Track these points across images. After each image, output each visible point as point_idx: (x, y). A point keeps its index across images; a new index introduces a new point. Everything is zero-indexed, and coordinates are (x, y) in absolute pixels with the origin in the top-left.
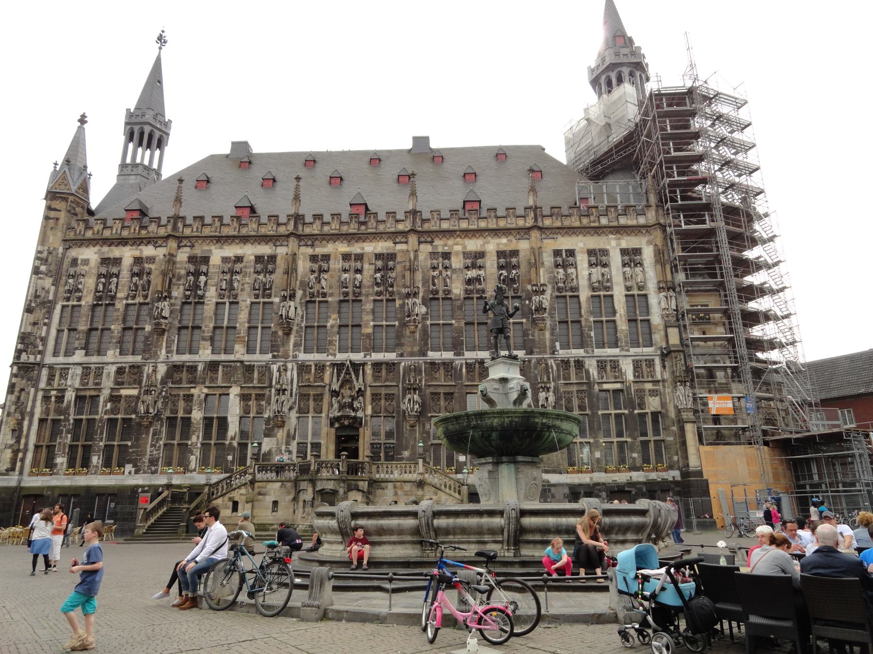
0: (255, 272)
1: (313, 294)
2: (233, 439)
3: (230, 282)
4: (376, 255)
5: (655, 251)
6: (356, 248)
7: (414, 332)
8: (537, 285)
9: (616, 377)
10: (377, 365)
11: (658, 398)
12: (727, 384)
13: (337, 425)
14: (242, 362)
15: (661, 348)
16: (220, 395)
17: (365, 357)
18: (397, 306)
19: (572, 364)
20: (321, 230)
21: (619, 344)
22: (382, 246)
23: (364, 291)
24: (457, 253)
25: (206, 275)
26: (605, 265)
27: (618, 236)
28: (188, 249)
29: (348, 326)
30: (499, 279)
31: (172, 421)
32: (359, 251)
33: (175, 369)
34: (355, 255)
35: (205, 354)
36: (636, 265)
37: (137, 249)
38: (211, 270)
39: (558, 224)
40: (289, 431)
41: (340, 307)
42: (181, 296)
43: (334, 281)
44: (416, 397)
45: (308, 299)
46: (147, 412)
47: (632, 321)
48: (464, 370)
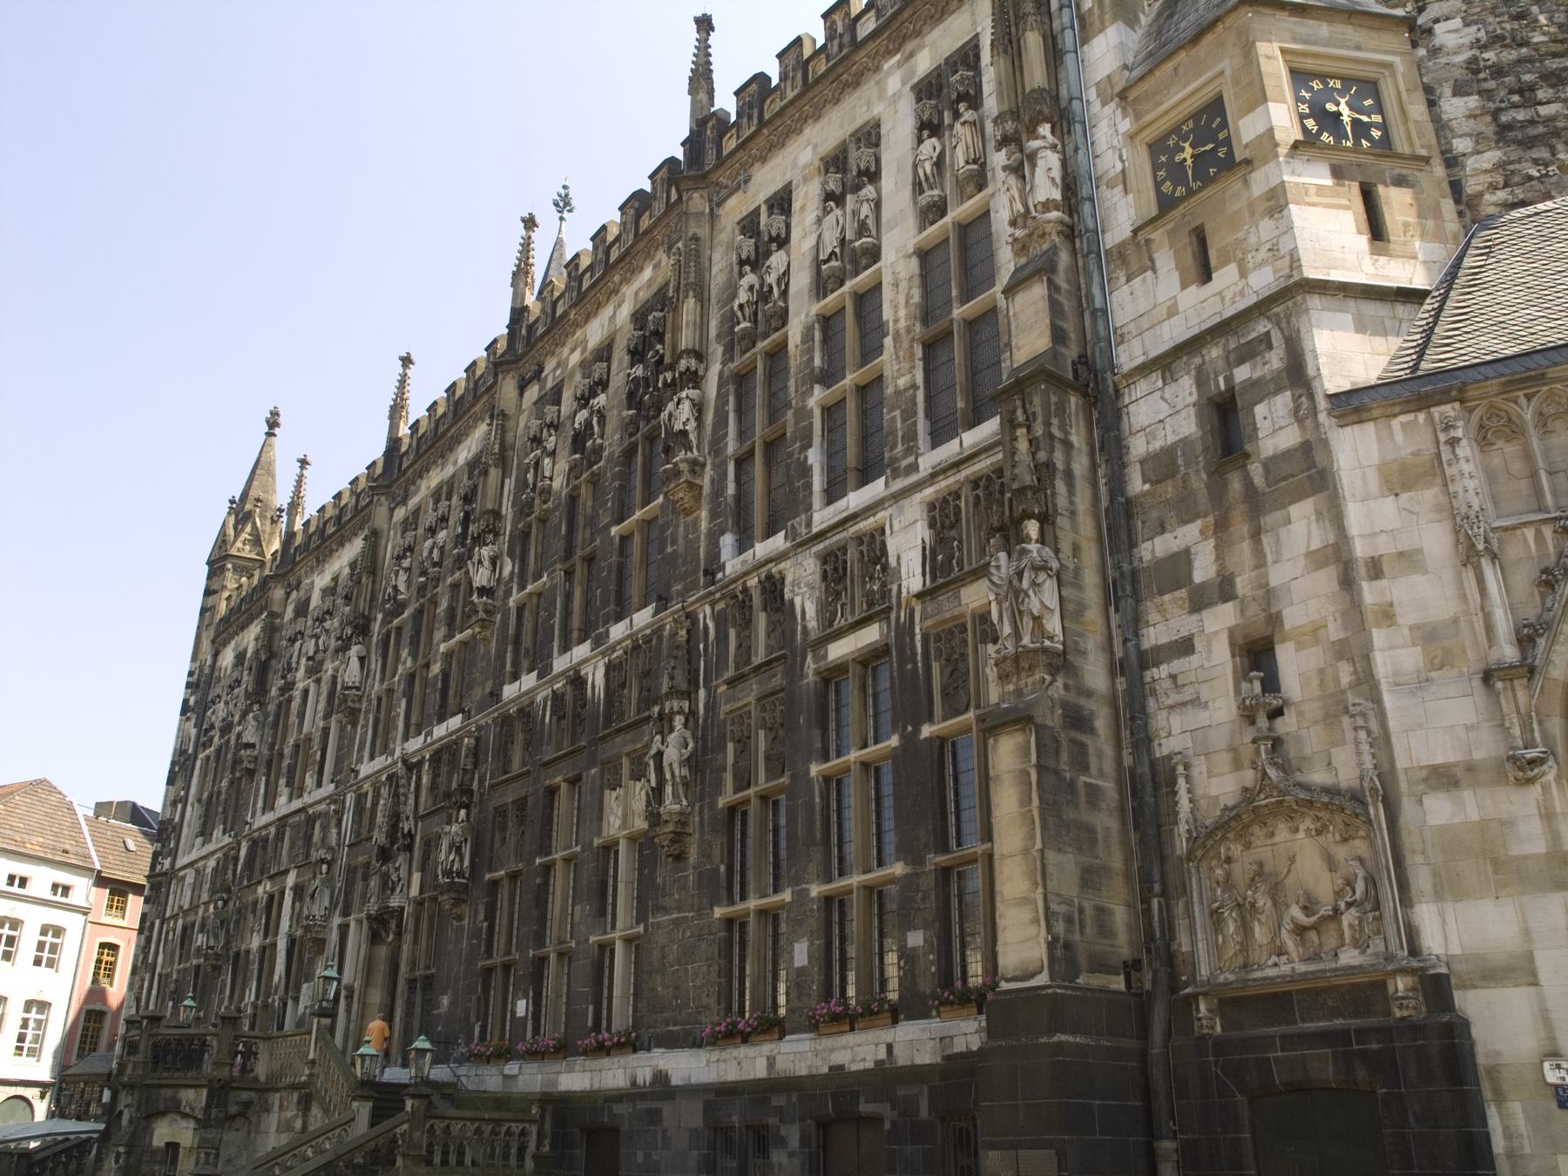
12: (1306, 448)
19: (757, 599)
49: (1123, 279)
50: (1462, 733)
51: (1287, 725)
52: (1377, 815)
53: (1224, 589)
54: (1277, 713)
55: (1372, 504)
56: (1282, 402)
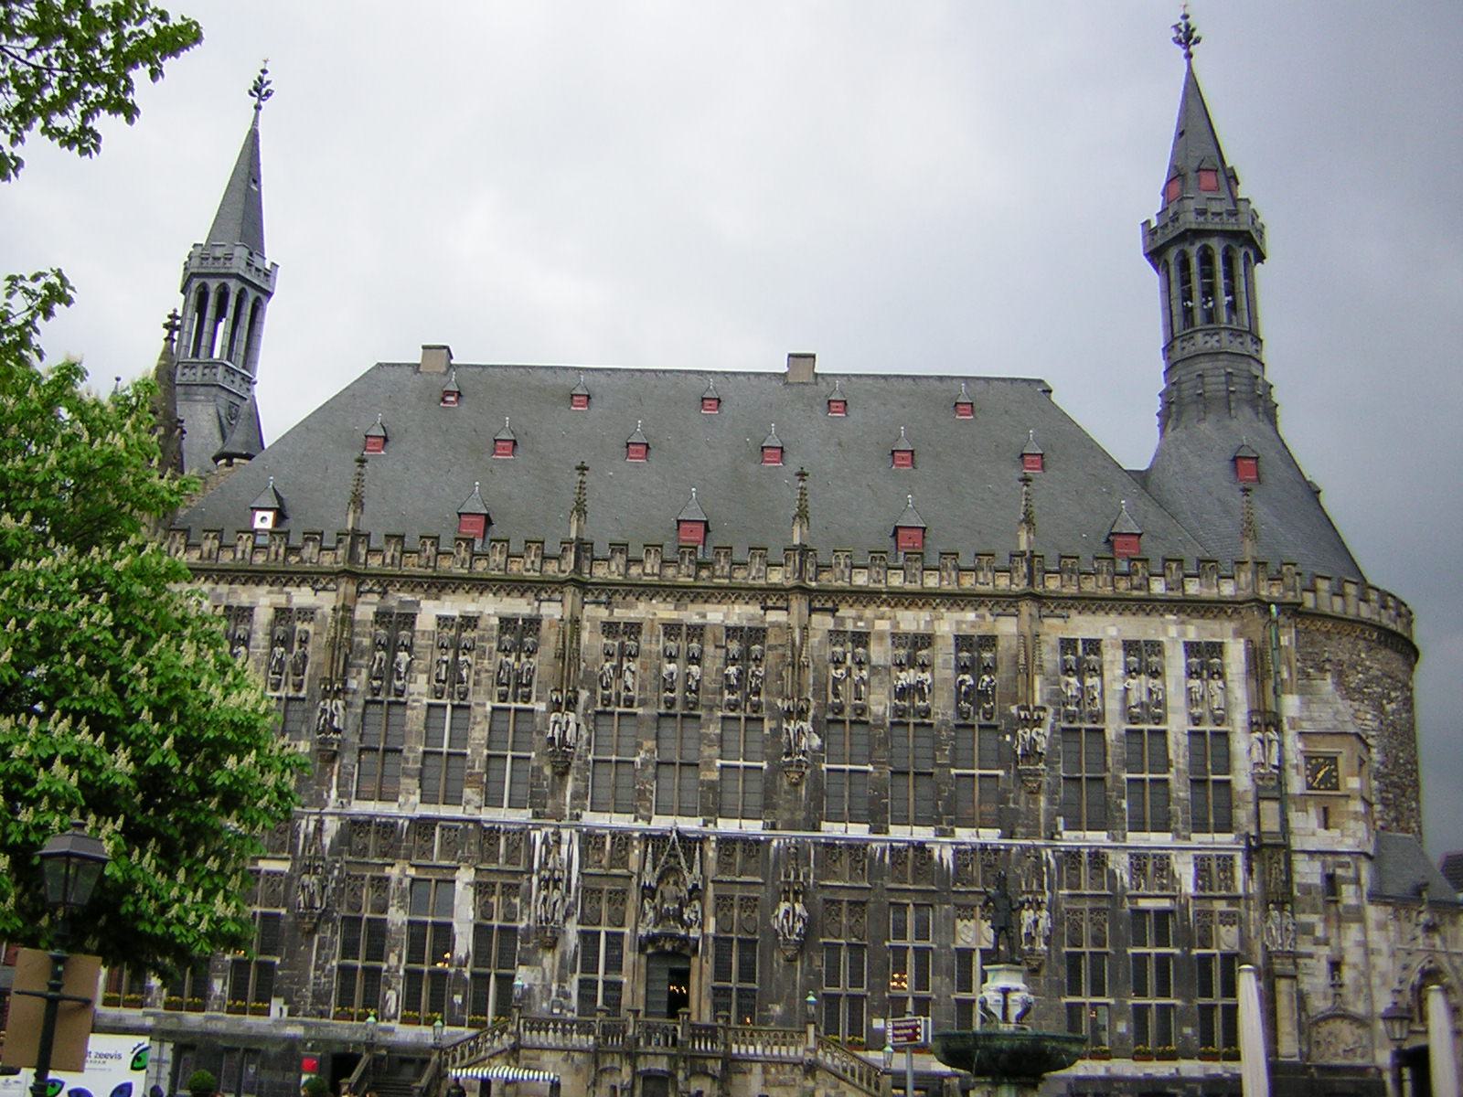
0: (499, 650)
1: (609, 700)
2: (463, 964)
3: (454, 667)
4: (728, 629)
5: (1247, 649)
6: (690, 615)
7: (797, 784)
8: (1027, 708)
9: (1162, 887)
10: (726, 842)
11: (1235, 929)
13: (650, 951)
14: (477, 822)
15: (1247, 836)
16: (437, 881)
17: (705, 825)
18: (767, 731)
19: (1085, 858)
20: (626, 575)
21: (1172, 826)
22: (740, 613)
23: (703, 698)
24: (881, 636)
25: (409, 649)
26: (1156, 674)
27: (1183, 617)
28: (376, 598)
29: (674, 764)
30: (958, 689)
31: (352, 923)
32: (696, 620)
33: (355, 826)
34: (689, 627)
35: (408, 806)
36: (1211, 676)
37: (281, 592)
38: (419, 641)
39: (1072, 590)
40: (563, 954)
41: (658, 728)
42: (363, 688)
43: (650, 674)
44: (799, 908)
45: (599, 708)
46: (312, 907)
47: (1198, 783)
48: (887, 859)
53: (1326, 942)
56: (1352, 888)
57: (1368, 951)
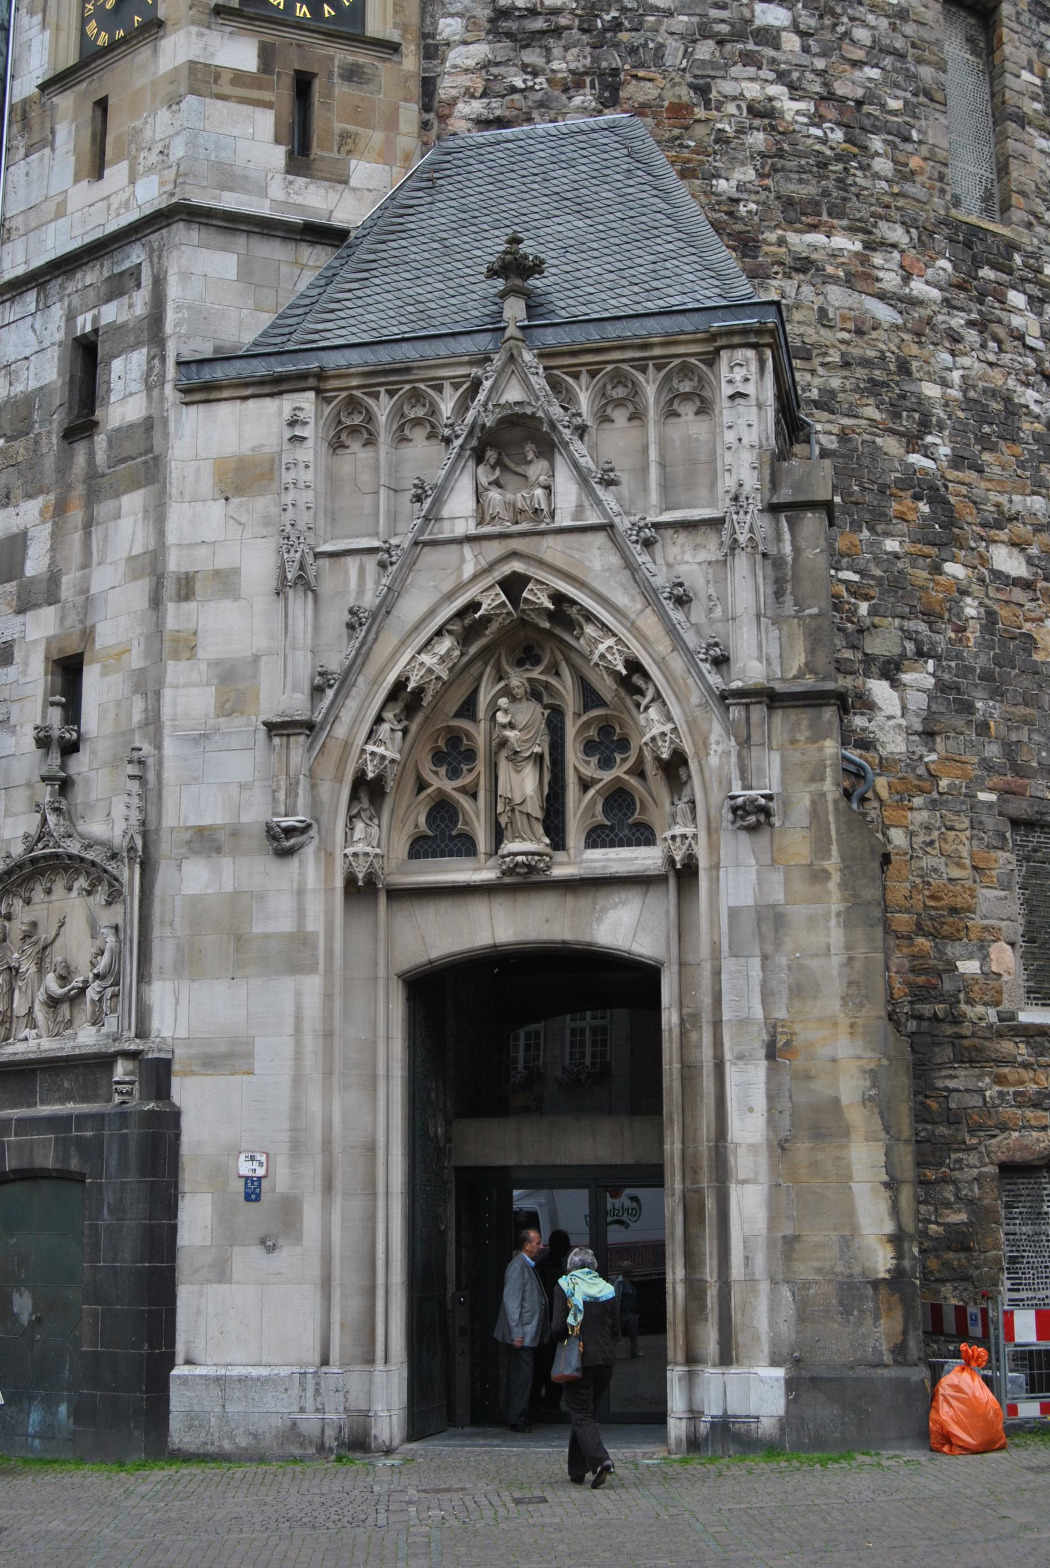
12: (148, 425)
49: (22, 151)
50: (234, 790)
51: (80, 764)
52: (131, 879)
54: (70, 748)
55: (199, 507)
57: (167, 586)
